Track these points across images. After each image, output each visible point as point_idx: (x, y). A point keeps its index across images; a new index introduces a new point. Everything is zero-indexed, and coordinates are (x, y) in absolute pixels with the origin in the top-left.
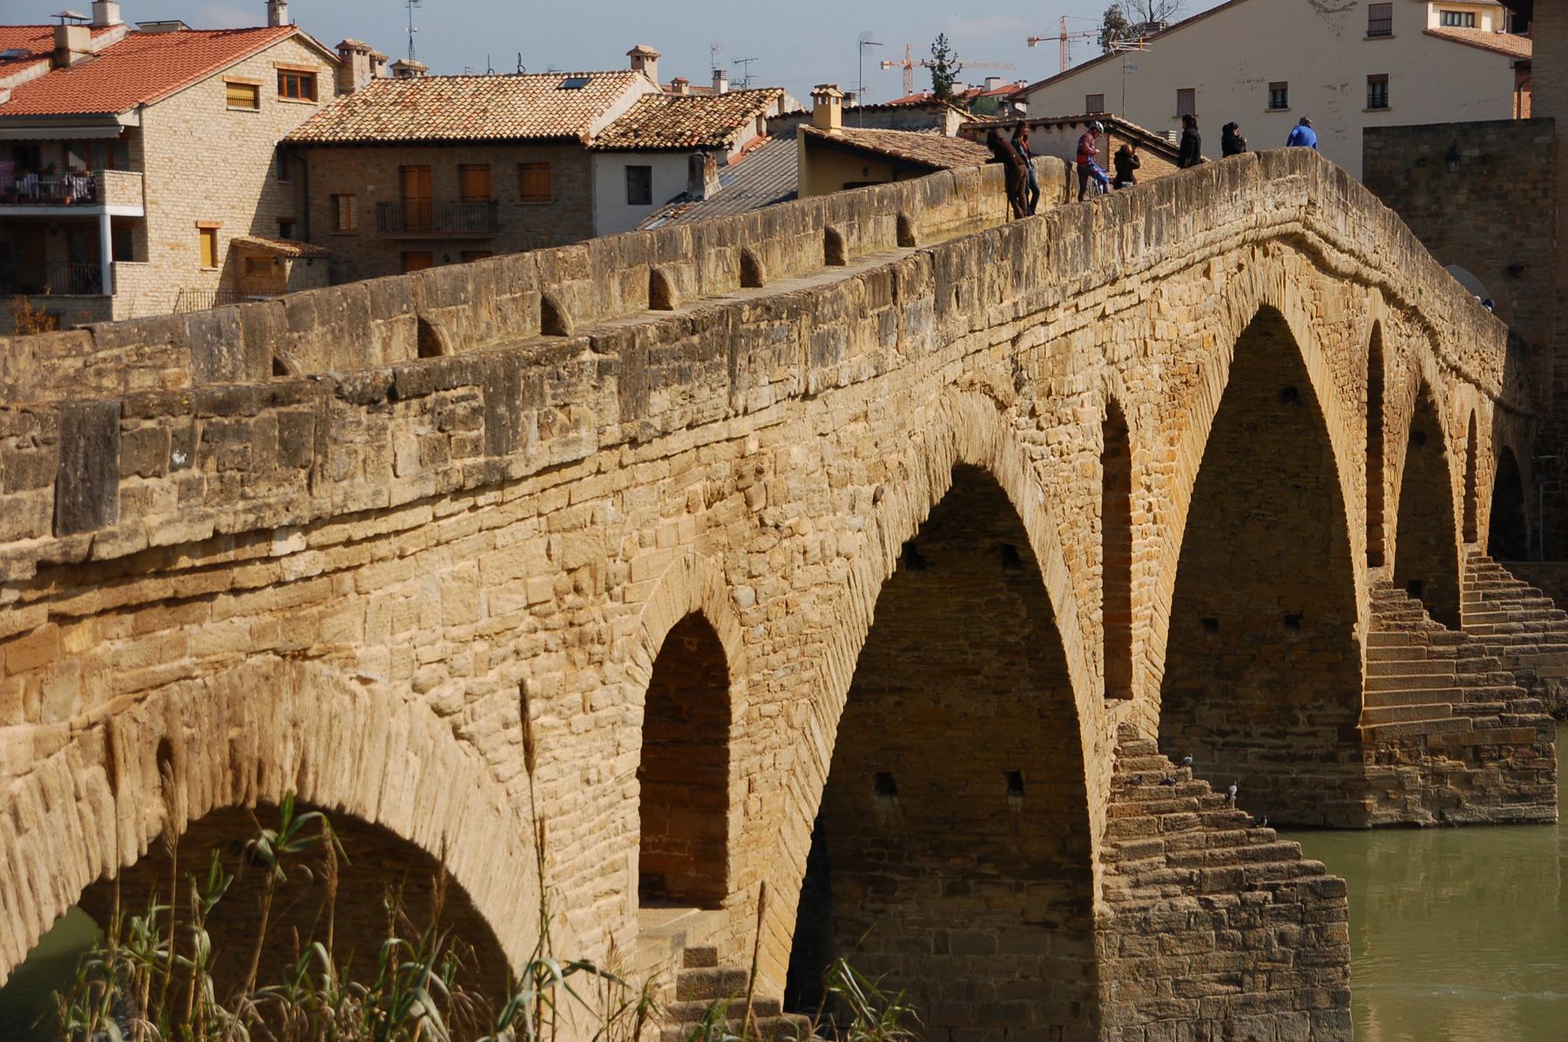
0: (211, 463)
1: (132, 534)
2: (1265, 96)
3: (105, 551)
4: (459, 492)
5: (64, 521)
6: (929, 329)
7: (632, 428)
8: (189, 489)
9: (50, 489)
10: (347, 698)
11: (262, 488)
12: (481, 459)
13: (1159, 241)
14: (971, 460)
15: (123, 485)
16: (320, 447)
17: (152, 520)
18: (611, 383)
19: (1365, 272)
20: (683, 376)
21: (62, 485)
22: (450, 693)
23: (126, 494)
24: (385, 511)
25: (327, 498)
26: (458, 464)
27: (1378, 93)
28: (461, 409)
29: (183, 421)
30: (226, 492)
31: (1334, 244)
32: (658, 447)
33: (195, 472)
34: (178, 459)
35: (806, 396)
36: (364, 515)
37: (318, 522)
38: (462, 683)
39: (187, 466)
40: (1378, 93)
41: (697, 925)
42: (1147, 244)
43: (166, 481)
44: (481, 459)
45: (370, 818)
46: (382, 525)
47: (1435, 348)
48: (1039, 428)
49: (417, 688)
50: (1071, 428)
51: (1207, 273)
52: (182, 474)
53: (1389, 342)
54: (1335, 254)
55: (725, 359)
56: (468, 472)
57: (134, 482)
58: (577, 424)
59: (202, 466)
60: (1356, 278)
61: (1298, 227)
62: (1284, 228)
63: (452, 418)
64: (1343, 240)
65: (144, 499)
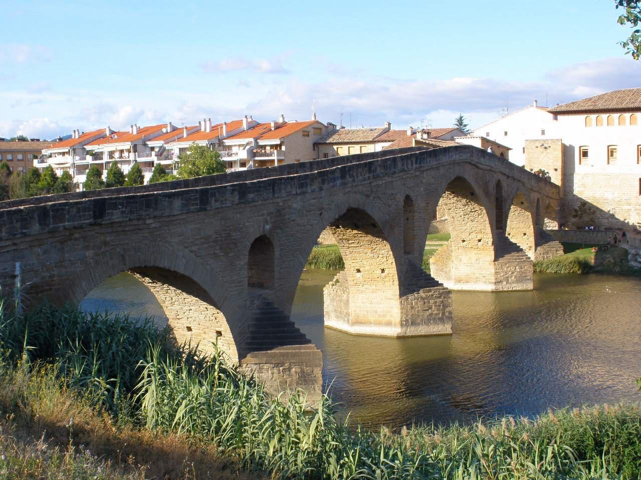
0: (128, 207)
1: (110, 219)
2: (541, 132)
3: (103, 222)
4: (192, 212)
5: (95, 217)
6: (338, 182)
7: (243, 201)
8: (123, 212)
9: (91, 213)
10: (167, 249)
11: (141, 212)
12: (198, 207)
13: (420, 163)
14: (353, 206)
15: (107, 211)
16: (156, 204)
17: (114, 217)
18: (236, 193)
19: (493, 169)
20: (258, 191)
21: (94, 212)
22: (194, 248)
23: (108, 213)
24: (173, 216)
25: (157, 213)
26: (192, 207)
27: (543, 132)
28: (192, 198)
29: (121, 201)
30: (132, 212)
31: (481, 164)
32: (252, 204)
33: (124, 209)
34: (120, 207)
35: (297, 194)
36: (168, 216)
37: (155, 217)
38: (197, 247)
39: (122, 208)
40: (543, 132)
41: (264, 292)
42: (416, 163)
43: (117, 211)
44: (198, 207)
45: (172, 269)
46: (173, 219)
47: (524, 185)
48: (381, 201)
49: (187, 248)
50: (393, 201)
51: (438, 169)
52: (121, 210)
53: (504, 183)
54: (482, 166)
55: (271, 188)
56: (195, 209)
57: (110, 211)
58: (226, 200)
59: (126, 208)
60: (491, 170)
61: (469, 161)
62: (463, 160)
63: (190, 199)
64: (483, 163)
65: (112, 214)
